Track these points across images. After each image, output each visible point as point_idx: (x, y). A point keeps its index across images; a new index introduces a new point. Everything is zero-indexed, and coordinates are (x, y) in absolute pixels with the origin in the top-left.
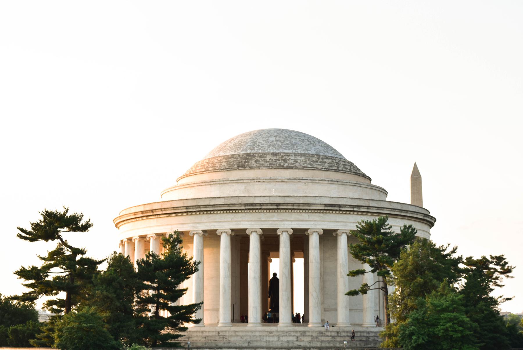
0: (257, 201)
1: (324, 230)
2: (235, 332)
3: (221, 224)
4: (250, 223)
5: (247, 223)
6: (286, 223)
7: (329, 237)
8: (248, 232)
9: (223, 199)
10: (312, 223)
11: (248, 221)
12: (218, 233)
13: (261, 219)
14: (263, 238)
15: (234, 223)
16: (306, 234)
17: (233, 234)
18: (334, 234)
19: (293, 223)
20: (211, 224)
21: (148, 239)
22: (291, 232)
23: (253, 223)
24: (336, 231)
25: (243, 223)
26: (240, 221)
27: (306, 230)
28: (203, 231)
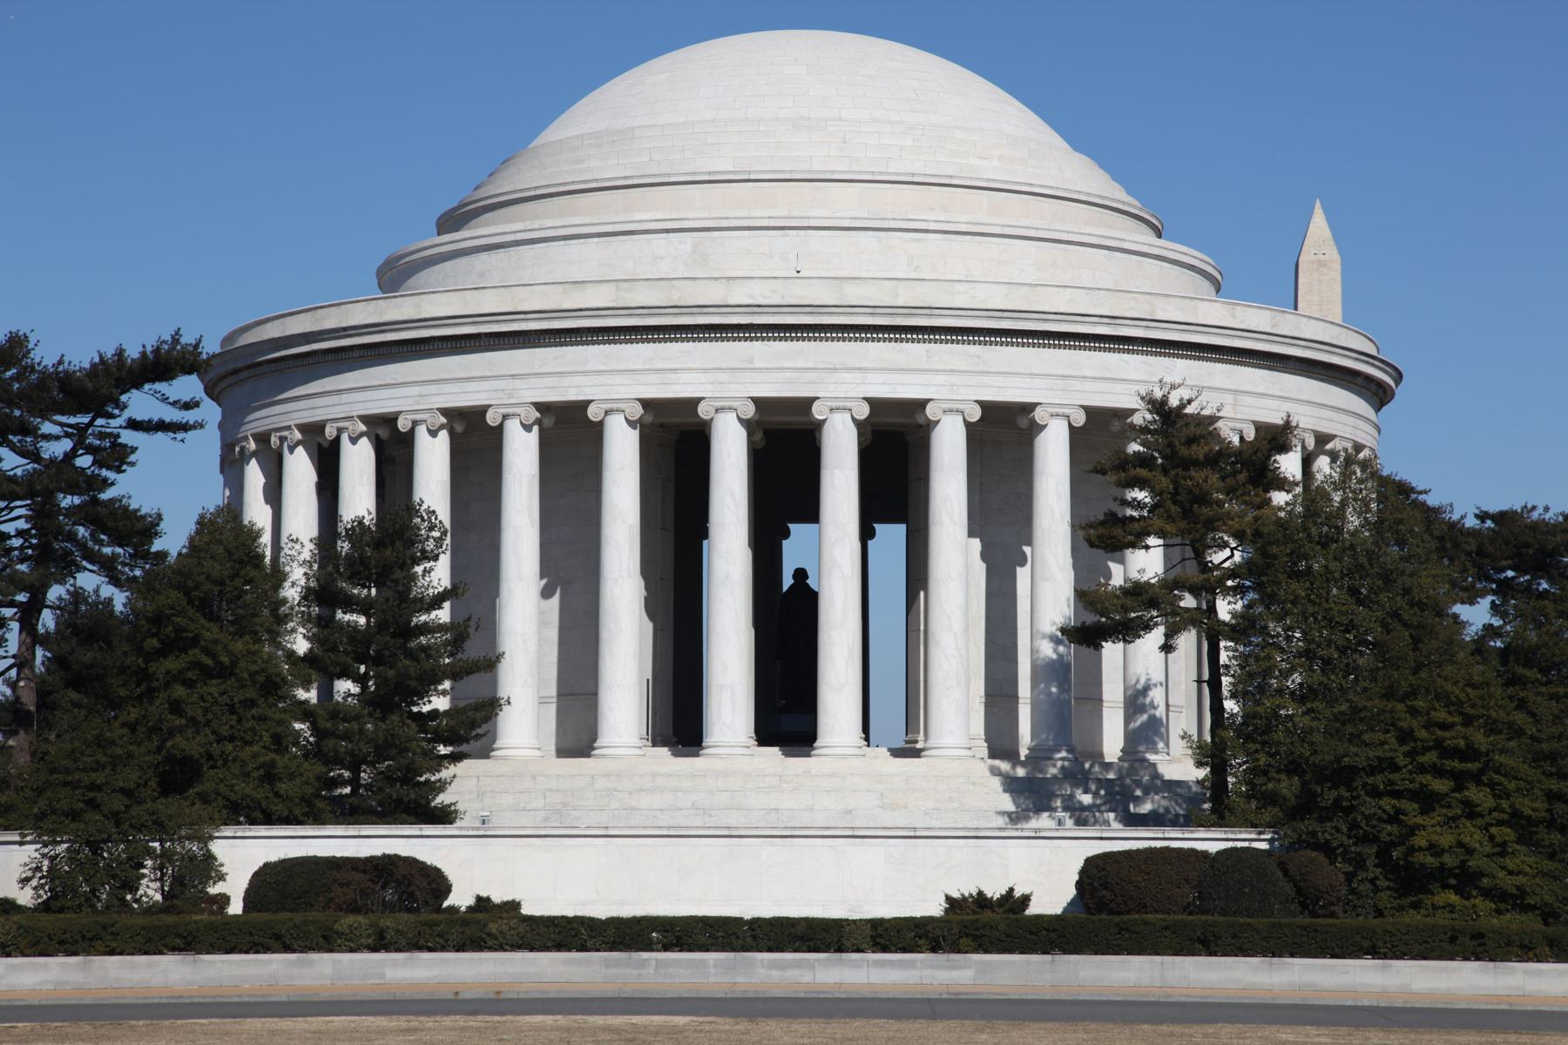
0: (739, 295)
1: (984, 405)
2: (654, 775)
3: (603, 379)
4: (711, 376)
5: (701, 376)
6: (848, 376)
7: (1003, 434)
8: (704, 411)
9: (612, 287)
10: (941, 379)
11: (705, 370)
12: (593, 413)
13: (751, 361)
14: (759, 436)
15: (654, 378)
16: (921, 420)
17: (649, 419)
18: (1023, 422)
19: (871, 377)
20: (568, 381)
21: (330, 432)
22: (863, 412)
23: (722, 377)
24: (1028, 408)
25: (685, 376)
26: (675, 370)
27: (921, 404)
28: (539, 406)
